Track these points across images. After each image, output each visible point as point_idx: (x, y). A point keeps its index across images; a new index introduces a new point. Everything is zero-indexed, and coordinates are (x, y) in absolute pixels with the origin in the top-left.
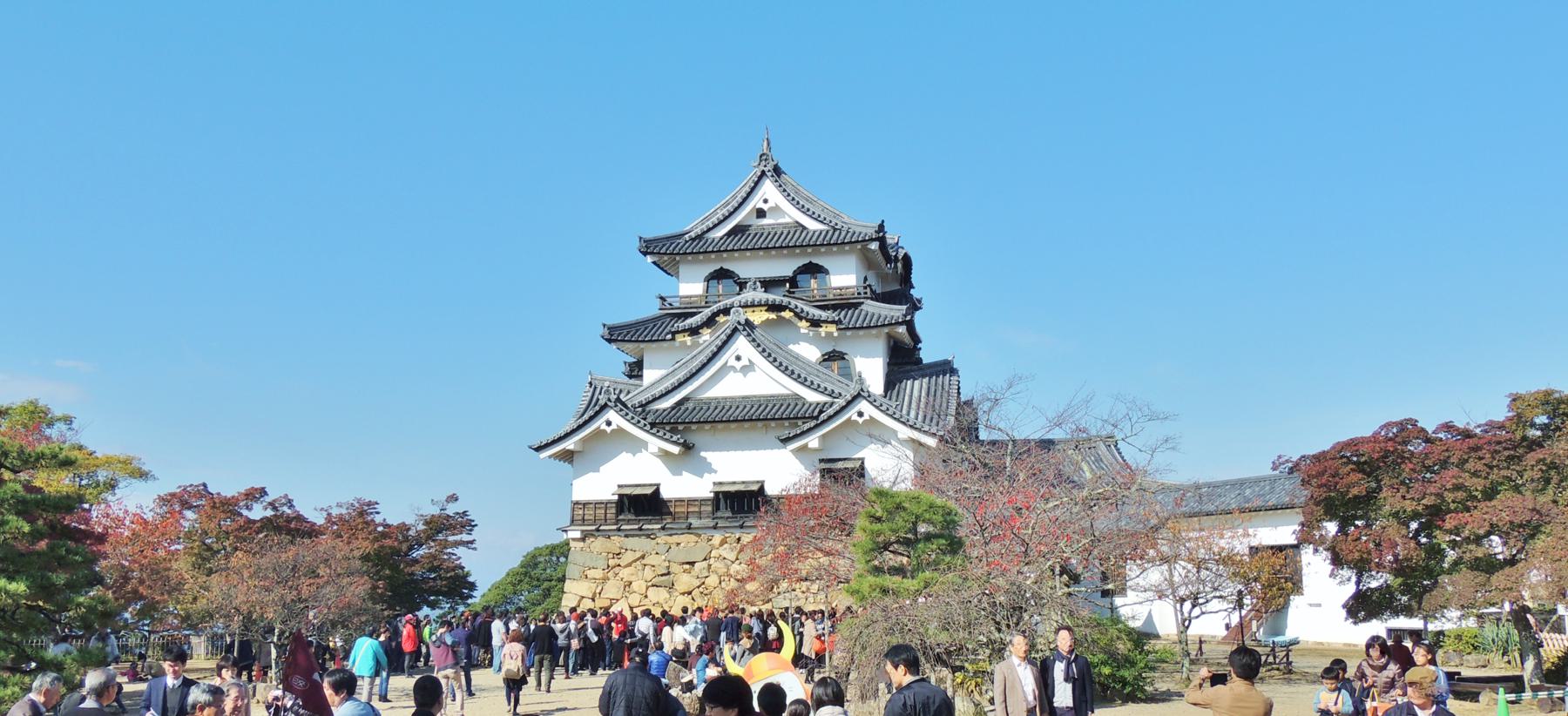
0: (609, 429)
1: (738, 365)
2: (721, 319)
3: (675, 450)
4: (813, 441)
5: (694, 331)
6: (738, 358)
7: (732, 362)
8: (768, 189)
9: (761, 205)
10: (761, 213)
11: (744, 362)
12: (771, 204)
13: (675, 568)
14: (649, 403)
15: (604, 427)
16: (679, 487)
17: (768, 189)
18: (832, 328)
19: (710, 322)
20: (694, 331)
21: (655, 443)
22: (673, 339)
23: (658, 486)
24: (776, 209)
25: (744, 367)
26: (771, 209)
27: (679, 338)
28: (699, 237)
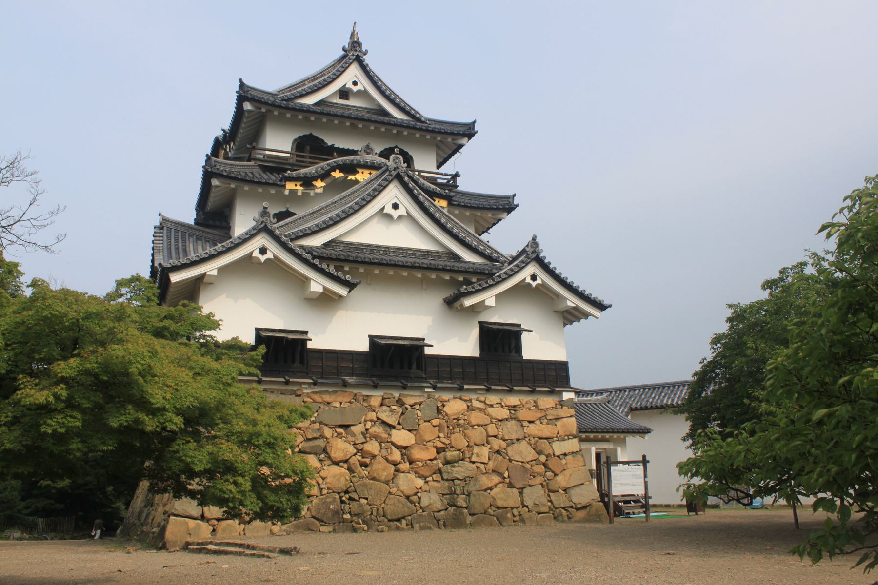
0: (263, 258)
1: (395, 214)
2: (337, 174)
3: (342, 291)
4: (489, 297)
5: (307, 182)
6: (395, 206)
7: (389, 210)
8: (353, 73)
9: (350, 85)
10: (344, 93)
11: (401, 211)
12: (359, 87)
13: (328, 432)
14: (299, 238)
15: (256, 254)
16: (323, 338)
17: (353, 73)
18: (444, 203)
19: (325, 175)
20: (307, 182)
21: (318, 284)
22: (284, 186)
23: (306, 333)
24: (364, 94)
25: (400, 217)
26: (359, 91)
27: (290, 186)
28: (290, 99)
